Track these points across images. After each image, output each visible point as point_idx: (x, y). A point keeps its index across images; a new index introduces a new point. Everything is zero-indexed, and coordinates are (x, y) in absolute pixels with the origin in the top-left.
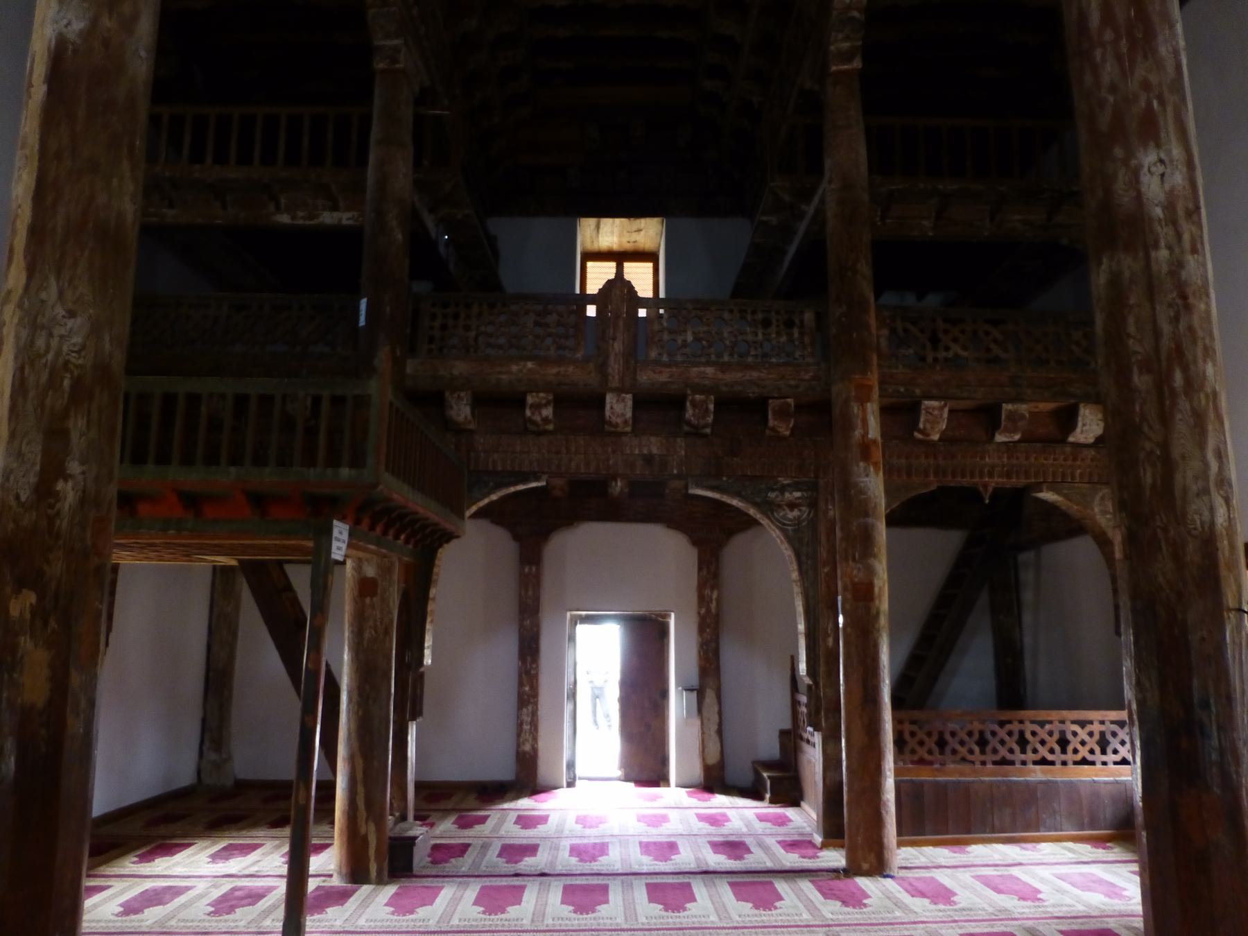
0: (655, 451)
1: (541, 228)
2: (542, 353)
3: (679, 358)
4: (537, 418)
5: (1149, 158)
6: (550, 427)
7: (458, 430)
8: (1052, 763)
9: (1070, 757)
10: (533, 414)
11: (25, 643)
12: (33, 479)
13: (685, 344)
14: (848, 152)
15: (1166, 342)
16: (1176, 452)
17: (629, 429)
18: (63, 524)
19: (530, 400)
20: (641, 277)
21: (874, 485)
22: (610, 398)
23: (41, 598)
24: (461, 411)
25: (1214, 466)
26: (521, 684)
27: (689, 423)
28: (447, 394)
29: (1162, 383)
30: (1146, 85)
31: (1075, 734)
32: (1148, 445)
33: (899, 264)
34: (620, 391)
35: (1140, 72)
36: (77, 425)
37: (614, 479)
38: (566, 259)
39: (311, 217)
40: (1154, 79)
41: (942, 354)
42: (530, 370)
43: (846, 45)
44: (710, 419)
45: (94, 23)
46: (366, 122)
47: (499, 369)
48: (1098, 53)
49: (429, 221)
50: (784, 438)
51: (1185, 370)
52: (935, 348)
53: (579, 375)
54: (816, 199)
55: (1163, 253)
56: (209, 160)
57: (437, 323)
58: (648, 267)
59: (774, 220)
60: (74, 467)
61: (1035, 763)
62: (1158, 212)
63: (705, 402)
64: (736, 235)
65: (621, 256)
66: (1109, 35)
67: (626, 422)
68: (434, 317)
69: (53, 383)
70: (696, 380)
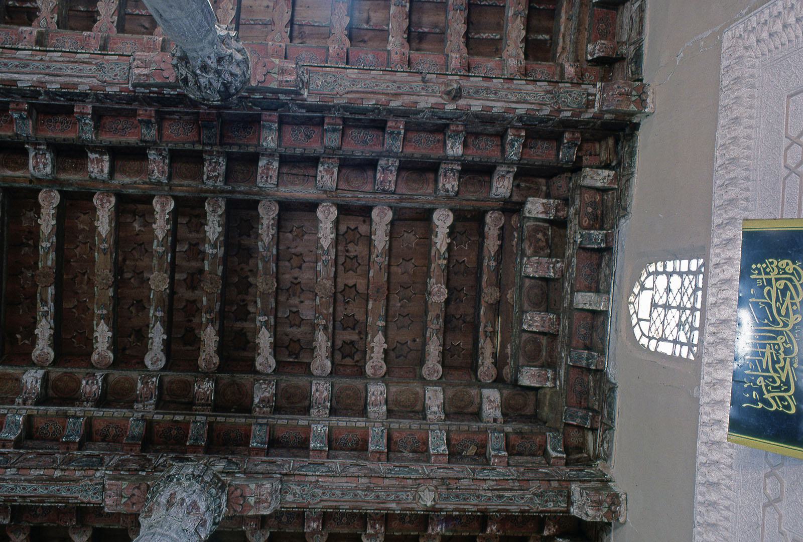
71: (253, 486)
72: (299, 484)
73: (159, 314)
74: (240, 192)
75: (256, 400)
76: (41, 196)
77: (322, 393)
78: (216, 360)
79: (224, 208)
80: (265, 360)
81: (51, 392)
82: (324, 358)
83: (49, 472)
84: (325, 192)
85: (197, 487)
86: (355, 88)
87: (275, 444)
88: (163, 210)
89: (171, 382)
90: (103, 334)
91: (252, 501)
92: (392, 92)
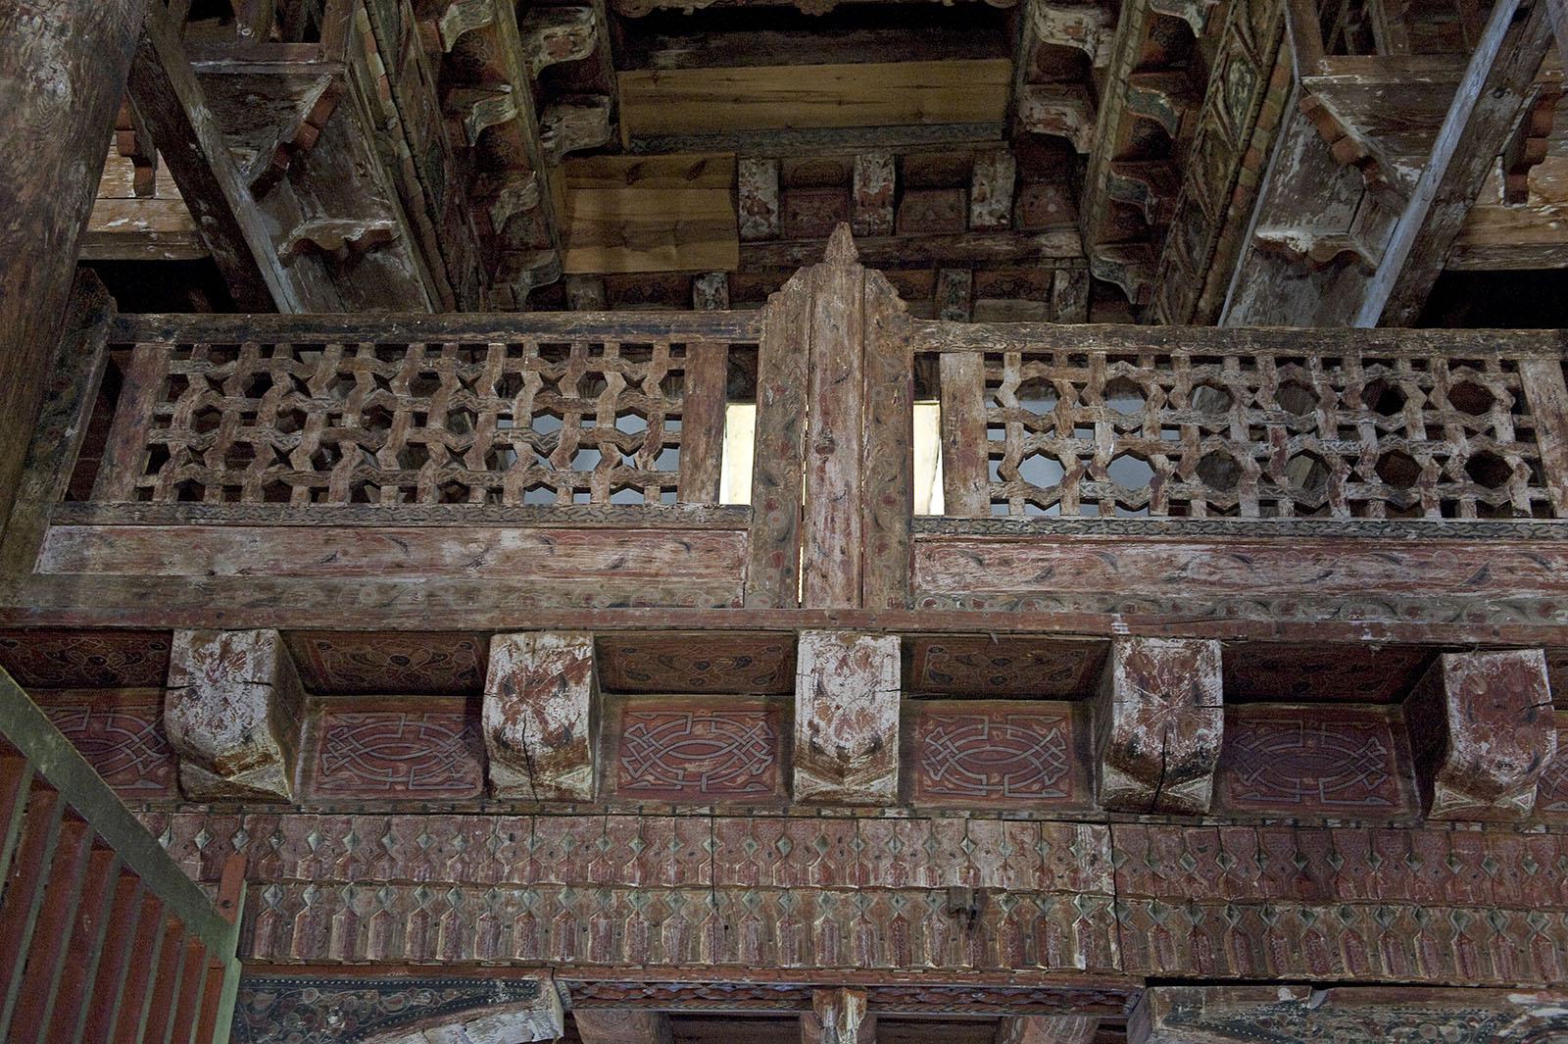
0: (991, 878)
2: (561, 499)
3: (1073, 513)
4: (528, 734)
6: (581, 780)
10: (511, 716)
17: (887, 784)
19: (502, 661)
22: (808, 648)
24: (227, 703)
27: (1127, 758)
28: (181, 641)
34: (853, 623)
37: (834, 992)
42: (508, 557)
44: (1212, 733)
47: (396, 554)
50: (1512, 824)
57: (184, 409)
63: (1186, 663)
67: (876, 747)
68: (177, 386)
70: (1143, 589)
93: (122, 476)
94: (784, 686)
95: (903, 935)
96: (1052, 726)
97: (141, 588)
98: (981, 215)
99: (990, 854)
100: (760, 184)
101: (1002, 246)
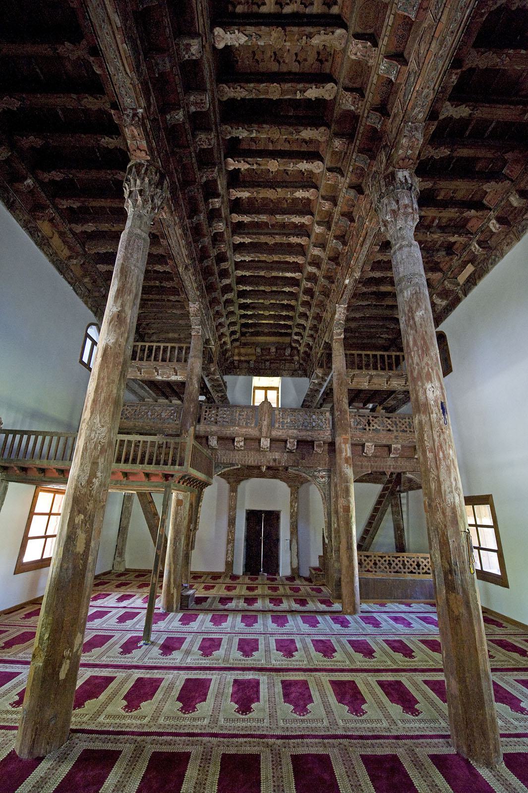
1: (241, 379)
5: (429, 386)
7: (213, 449)
8: (415, 573)
9: (421, 571)
11: (79, 531)
12: (87, 478)
13: (287, 423)
14: (339, 361)
15: (437, 444)
16: (441, 479)
18: (94, 493)
19: (236, 440)
20: (272, 396)
21: (349, 472)
23: (85, 517)
24: (213, 442)
25: (454, 483)
26: (228, 536)
29: (436, 457)
30: (427, 364)
31: (423, 562)
32: (433, 476)
33: (357, 396)
34: (266, 437)
35: (426, 359)
36: (101, 461)
38: (249, 391)
39: (168, 377)
40: (429, 362)
41: (371, 428)
43: (339, 331)
44: (295, 447)
45: (117, 340)
46: (188, 348)
48: (413, 353)
49: (206, 379)
51: (443, 453)
52: (369, 426)
53: (253, 432)
54: (330, 376)
55: (435, 415)
56: (137, 359)
58: (275, 392)
59: (316, 381)
60: (99, 474)
61: (409, 573)
62: (432, 402)
64: (305, 383)
65: (267, 389)
66: (415, 349)
68: (206, 412)
69: (95, 448)
71: (401, 152)
72: (413, 108)
73: (292, 165)
74: (215, 118)
75: (353, 108)
76: (234, 221)
77: (358, 49)
78: (322, 129)
79: (227, 126)
80: (326, 92)
81: (327, 220)
82: (332, 37)
83: (360, 242)
84: (203, 47)
85: (385, 200)
86: (121, 68)
87: (383, 109)
88: (233, 165)
89: (331, 162)
90: (300, 194)
91: (410, 152)
92: (109, 28)
93: (202, 420)
94: (260, 442)
95: (269, 462)
96: (283, 444)
97: (205, 432)
98: (286, 354)
99: (277, 455)
100: (259, 350)
101: (289, 358)
